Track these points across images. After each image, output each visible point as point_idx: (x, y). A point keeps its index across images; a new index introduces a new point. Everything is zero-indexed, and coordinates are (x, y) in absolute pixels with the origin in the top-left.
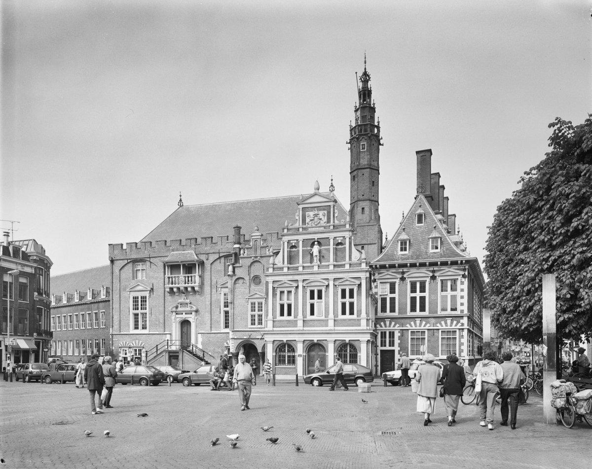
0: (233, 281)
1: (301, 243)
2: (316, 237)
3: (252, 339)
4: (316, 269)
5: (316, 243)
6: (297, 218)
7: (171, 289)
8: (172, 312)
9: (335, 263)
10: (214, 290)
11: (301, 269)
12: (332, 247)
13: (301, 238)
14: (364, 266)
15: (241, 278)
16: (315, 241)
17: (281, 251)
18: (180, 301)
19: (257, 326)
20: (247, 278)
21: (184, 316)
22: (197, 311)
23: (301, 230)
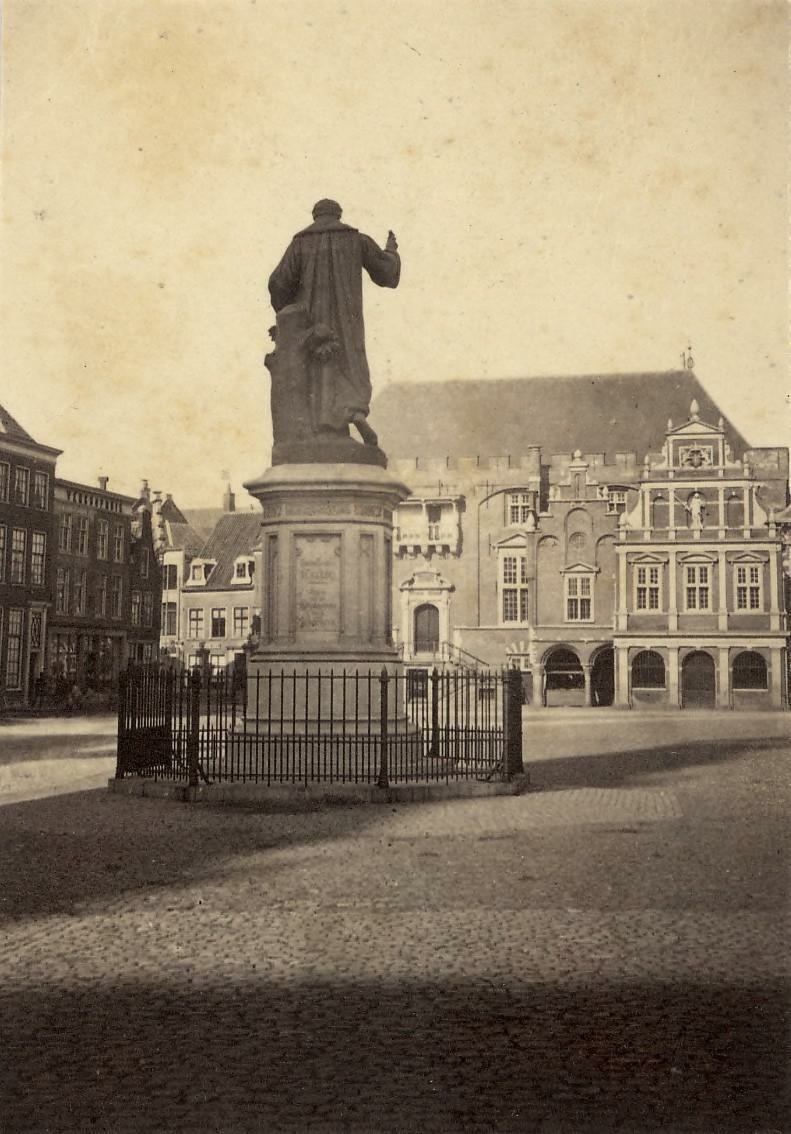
0: (536, 540)
1: (672, 496)
2: (696, 485)
3: (573, 642)
4: (697, 536)
5: (697, 495)
6: (664, 454)
7: (403, 549)
8: (402, 590)
9: (727, 527)
10: (484, 551)
11: (672, 536)
12: (721, 502)
13: (672, 486)
14: (772, 533)
15: (551, 536)
16: (695, 493)
17: (640, 502)
18: (417, 570)
19: (579, 620)
20: (562, 538)
21: (425, 598)
22: (452, 589)
23: (671, 475)
